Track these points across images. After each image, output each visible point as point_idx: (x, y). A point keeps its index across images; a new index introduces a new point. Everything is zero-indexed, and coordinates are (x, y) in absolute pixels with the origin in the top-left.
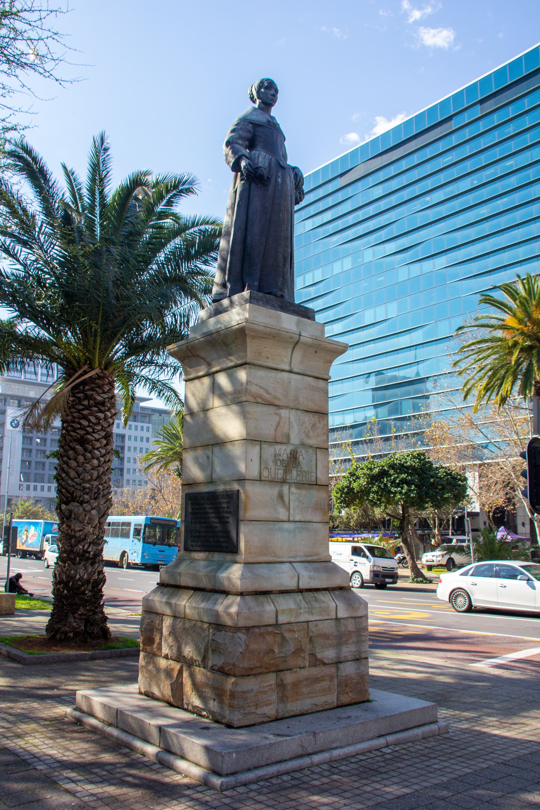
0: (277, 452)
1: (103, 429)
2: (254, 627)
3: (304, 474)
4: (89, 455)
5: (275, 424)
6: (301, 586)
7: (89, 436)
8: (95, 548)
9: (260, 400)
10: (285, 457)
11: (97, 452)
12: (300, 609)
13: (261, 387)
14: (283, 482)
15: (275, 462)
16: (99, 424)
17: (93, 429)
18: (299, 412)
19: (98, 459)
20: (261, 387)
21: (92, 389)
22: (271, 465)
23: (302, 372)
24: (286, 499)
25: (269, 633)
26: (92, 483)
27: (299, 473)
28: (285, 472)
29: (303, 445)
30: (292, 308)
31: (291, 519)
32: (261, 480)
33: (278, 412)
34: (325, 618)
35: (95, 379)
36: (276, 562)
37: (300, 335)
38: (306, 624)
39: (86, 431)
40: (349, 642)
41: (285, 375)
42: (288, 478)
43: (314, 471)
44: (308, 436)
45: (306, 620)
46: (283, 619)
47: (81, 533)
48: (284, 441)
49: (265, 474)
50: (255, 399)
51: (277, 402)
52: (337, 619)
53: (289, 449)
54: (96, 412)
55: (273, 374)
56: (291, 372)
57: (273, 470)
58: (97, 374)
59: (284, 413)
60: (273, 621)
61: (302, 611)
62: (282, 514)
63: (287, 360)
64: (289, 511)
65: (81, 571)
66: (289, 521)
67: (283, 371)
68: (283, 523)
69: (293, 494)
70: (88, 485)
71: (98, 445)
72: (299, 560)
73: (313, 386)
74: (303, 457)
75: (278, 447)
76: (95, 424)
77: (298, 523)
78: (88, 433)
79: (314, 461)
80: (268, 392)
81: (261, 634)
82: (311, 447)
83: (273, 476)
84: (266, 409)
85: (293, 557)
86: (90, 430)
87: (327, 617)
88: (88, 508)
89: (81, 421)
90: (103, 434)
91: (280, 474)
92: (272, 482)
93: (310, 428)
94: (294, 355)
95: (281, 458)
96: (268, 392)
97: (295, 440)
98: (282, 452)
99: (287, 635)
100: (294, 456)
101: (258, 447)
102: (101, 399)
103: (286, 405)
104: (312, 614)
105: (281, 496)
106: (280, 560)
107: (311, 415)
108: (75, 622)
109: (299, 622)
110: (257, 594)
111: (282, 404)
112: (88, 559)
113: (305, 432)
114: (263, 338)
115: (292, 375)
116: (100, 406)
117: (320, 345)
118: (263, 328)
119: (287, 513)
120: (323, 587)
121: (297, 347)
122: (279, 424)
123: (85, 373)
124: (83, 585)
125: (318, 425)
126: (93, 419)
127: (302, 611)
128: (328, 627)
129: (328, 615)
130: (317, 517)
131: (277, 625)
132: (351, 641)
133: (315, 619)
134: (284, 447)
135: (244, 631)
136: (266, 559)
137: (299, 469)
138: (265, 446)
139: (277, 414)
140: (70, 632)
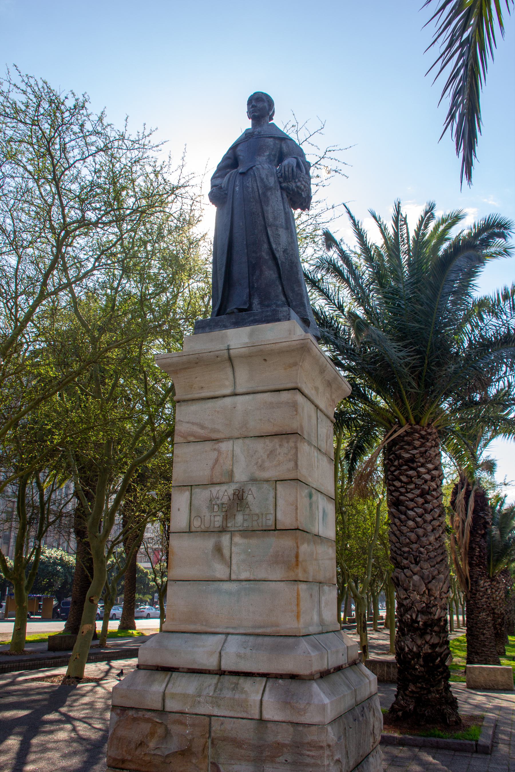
1: (417, 487)
2: (132, 708)
3: (255, 518)
4: (403, 517)
5: (211, 463)
6: (224, 667)
7: (402, 498)
8: (424, 618)
9: (192, 439)
10: (225, 500)
11: (411, 513)
12: (200, 696)
13: (193, 424)
14: (223, 530)
15: (211, 508)
16: (412, 482)
17: (406, 489)
18: (247, 441)
19: (414, 520)
20: (193, 424)
21: (401, 448)
22: (205, 512)
23: (250, 390)
24: (226, 552)
25: (148, 720)
26: (411, 546)
27: (246, 517)
28: (226, 518)
29: (254, 480)
30: (252, 318)
31: (233, 577)
32: (190, 532)
33: (216, 446)
34: (236, 715)
36: (206, 633)
37: (228, 349)
38: (207, 719)
39: (400, 492)
40: (277, 760)
41: (228, 401)
43: (272, 512)
44: (261, 467)
45: (207, 712)
46: (171, 705)
47: (408, 601)
48: (224, 480)
49: (196, 523)
50: (185, 438)
51: (215, 436)
52: (261, 720)
53: (230, 490)
54: (406, 470)
55: (210, 404)
56: (236, 395)
57: (207, 518)
58: (406, 431)
59: (224, 446)
60: (158, 706)
61: (202, 699)
62: (219, 570)
64: (230, 567)
65: (409, 642)
66: (230, 580)
67: (224, 396)
68: (221, 583)
69: (237, 546)
70: (406, 549)
71: (411, 504)
72: (242, 631)
73: (271, 403)
74: (253, 497)
75: (215, 490)
76: (407, 483)
77: (244, 583)
78: (402, 494)
79: (271, 499)
80: (203, 427)
81: (135, 719)
82: (267, 481)
83: (207, 525)
84: (199, 447)
85: (233, 628)
86: (403, 490)
87: (244, 715)
88: (409, 573)
89: (394, 483)
90: (418, 492)
91: (218, 521)
92: (207, 532)
93: (265, 457)
94: (237, 374)
95: (218, 502)
96: (203, 427)
97: (241, 475)
99: (175, 729)
100: (239, 499)
101: (187, 494)
102: (409, 455)
103: (228, 436)
104: (219, 706)
105: (218, 549)
106: (213, 630)
107: (267, 440)
108: (403, 699)
109: (196, 714)
110: (157, 670)
112: (418, 628)
113: (257, 463)
114: (186, 368)
116: (410, 464)
117: (261, 351)
118: (177, 359)
119: (227, 571)
120: (261, 671)
121: (235, 364)
123: (395, 431)
124: (413, 659)
125: (279, 450)
126: (404, 478)
127: (202, 699)
128: (245, 731)
129: (246, 712)
130: (278, 573)
131: (162, 712)
132: (281, 759)
133: (222, 714)
134: (224, 488)
135: (119, 711)
136: (192, 627)
137: (247, 511)
138: (196, 490)
139: (215, 449)
140: (400, 710)
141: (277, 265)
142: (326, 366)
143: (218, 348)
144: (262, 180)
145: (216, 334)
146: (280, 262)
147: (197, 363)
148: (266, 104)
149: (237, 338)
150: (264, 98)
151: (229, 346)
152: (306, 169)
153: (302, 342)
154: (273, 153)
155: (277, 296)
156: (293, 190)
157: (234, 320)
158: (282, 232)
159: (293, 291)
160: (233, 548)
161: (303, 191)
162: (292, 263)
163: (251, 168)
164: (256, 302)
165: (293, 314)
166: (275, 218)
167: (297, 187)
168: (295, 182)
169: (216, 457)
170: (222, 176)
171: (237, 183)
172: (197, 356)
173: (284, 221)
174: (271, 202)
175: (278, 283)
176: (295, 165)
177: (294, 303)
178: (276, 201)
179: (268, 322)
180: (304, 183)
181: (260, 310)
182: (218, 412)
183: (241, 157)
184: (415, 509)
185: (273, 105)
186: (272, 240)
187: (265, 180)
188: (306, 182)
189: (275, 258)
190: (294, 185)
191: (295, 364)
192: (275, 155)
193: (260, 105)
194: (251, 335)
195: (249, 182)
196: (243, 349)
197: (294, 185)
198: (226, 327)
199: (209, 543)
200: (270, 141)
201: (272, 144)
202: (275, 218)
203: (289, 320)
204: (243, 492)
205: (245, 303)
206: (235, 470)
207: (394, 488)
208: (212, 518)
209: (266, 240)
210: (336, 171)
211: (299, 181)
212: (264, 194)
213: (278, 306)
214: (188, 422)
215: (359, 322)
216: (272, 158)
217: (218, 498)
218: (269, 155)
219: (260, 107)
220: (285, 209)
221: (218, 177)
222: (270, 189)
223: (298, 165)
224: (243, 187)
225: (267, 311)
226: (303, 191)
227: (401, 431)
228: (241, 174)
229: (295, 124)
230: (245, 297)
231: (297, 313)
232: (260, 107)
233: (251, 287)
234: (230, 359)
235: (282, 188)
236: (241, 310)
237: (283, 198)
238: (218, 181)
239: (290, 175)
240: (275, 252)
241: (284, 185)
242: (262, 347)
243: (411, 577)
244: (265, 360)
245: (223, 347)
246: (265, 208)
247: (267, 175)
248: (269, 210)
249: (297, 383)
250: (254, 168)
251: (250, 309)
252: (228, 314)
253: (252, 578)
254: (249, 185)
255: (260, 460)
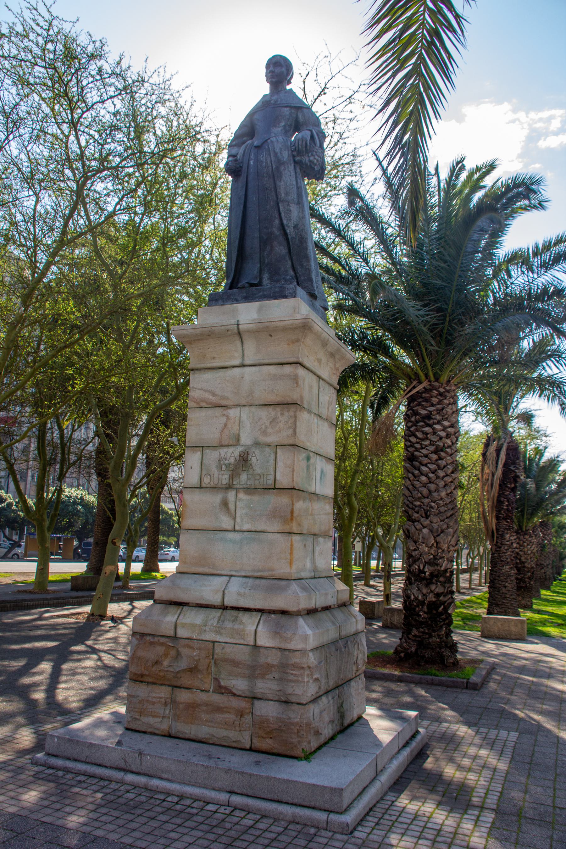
0: (223, 456)
2: (150, 635)
3: (258, 477)
4: (416, 472)
5: (220, 427)
6: (227, 603)
8: (431, 568)
9: (204, 404)
10: (232, 460)
11: (424, 469)
12: (205, 626)
13: (205, 391)
14: (229, 487)
15: (219, 467)
16: (427, 438)
17: (421, 444)
18: (253, 409)
19: (426, 476)
20: (205, 391)
21: (419, 404)
22: (214, 470)
24: (232, 506)
25: (162, 644)
26: (423, 500)
27: (250, 476)
28: (232, 477)
29: (257, 444)
30: (261, 294)
31: (237, 528)
32: (201, 488)
33: (225, 412)
35: (422, 393)
38: (211, 644)
39: (416, 448)
40: (267, 677)
41: (237, 371)
42: (235, 483)
43: (273, 473)
44: (265, 433)
45: (211, 639)
46: (182, 633)
47: (417, 552)
48: (231, 443)
49: (206, 480)
50: (198, 403)
51: (224, 403)
52: (255, 646)
53: (237, 451)
54: (422, 427)
55: (221, 373)
56: (243, 366)
57: (216, 476)
58: (424, 388)
59: (233, 413)
60: (171, 633)
62: (226, 522)
63: (238, 354)
65: (415, 591)
66: (234, 530)
67: (234, 367)
68: (227, 533)
69: (241, 502)
70: (418, 503)
71: (425, 460)
72: (243, 574)
74: (256, 459)
75: (223, 451)
76: (422, 440)
77: (246, 533)
78: (417, 450)
79: (272, 461)
80: (214, 394)
81: (152, 643)
82: (269, 445)
83: (216, 482)
84: (210, 412)
85: (235, 571)
86: (418, 446)
88: (419, 526)
90: (432, 448)
91: (225, 479)
92: (215, 488)
93: (268, 424)
94: (246, 347)
95: (226, 462)
96: (214, 394)
97: (246, 439)
98: (228, 455)
99: (185, 651)
100: (244, 460)
101: (199, 454)
103: (236, 403)
104: (221, 634)
105: (225, 504)
106: (218, 572)
107: (270, 409)
108: (406, 642)
109: (202, 640)
110: (171, 604)
111: (231, 403)
112: (424, 578)
113: (260, 429)
114: (199, 340)
115: (246, 368)
117: (267, 327)
118: (191, 331)
119: (232, 522)
120: (258, 607)
122: (226, 425)
123: (414, 387)
125: (280, 418)
126: (419, 435)
128: (242, 654)
129: (244, 640)
130: (275, 526)
131: (175, 638)
132: (271, 676)
134: (231, 450)
135: (138, 637)
136: (201, 570)
137: (251, 471)
138: (207, 451)
139: (224, 415)
140: (402, 652)
141: (287, 239)
142: (328, 340)
143: (228, 322)
144: (276, 154)
145: (228, 307)
146: (290, 238)
147: (209, 335)
148: (284, 69)
149: (247, 313)
150: (282, 62)
151: (238, 321)
152: (320, 141)
153: (304, 321)
154: (289, 123)
155: (286, 271)
156: (306, 165)
157: (245, 294)
158: (294, 208)
159: (302, 266)
160: (238, 503)
161: (316, 165)
162: (302, 238)
163: (266, 141)
164: (266, 277)
165: (300, 291)
166: (287, 194)
167: (310, 161)
168: (309, 157)
169: (225, 421)
170: (239, 145)
171: (252, 157)
172: (209, 329)
173: (295, 196)
174: (283, 177)
175: (287, 258)
176: (309, 139)
177: (302, 278)
178: (289, 174)
179: (276, 298)
180: (317, 157)
181: (269, 286)
182: (228, 381)
183: (258, 127)
184: (429, 465)
185: (292, 68)
186: (283, 215)
187: (279, 154)
188: (319, 156)
189: (285, 234)
190: (307, 159)
191: (298, 340)
192: (291, 125)
193: (278, 70)
194: (260, 310)
195: (263, 157)
196: (251, 325)
197: (307, 159)
198: (237, 301)
199: (217, 498)
200: (286, 111)
201: (288, 113)
202: (287, 194)
203: (295, 297)
204: (248, 454)
205: (256, 278)
206: (241, 434)
207: (409, 444)
208: (220, 476)
209: (277, 216)
210: (371, 107)
211: (312, 155)
212: (278, 169)
213: (286, 281)
214: (200, 389)
215: (376, 284)
216: (288, 128)
217: (226, 459)
218: (285, 126)
219: (279, 70)
220: (297, 183)
221: (235, 145)
222: (284, 163)
223: (312, 137)
224: (257, 161)
225: (275, 288)
226: (316, 165)
227: (420, 388)
228: (256, 147)
229: (328, 54)
230: (256, 272)
231: (303, 288)
232: (279, 70)
233: (261, 262)
234: (239, 333)
235: (295, 162)
236: (252, 285)
237: (296, 173)
238: (234, 151)
239: (304, 149)
240: (286, 228)
241: (298, 158)
242: (268, 324)
243: (421, 530)
244: (271, 335)
245: (233, 322)
246: (278, 183)
247: (281, 149)
248: (281, 185)
249: (298, 358)
250: (269, 141)
251: (260, 284)
252: (240, 288)
253: (253, 529)
254: (263, 159)
255: (263, 427)
